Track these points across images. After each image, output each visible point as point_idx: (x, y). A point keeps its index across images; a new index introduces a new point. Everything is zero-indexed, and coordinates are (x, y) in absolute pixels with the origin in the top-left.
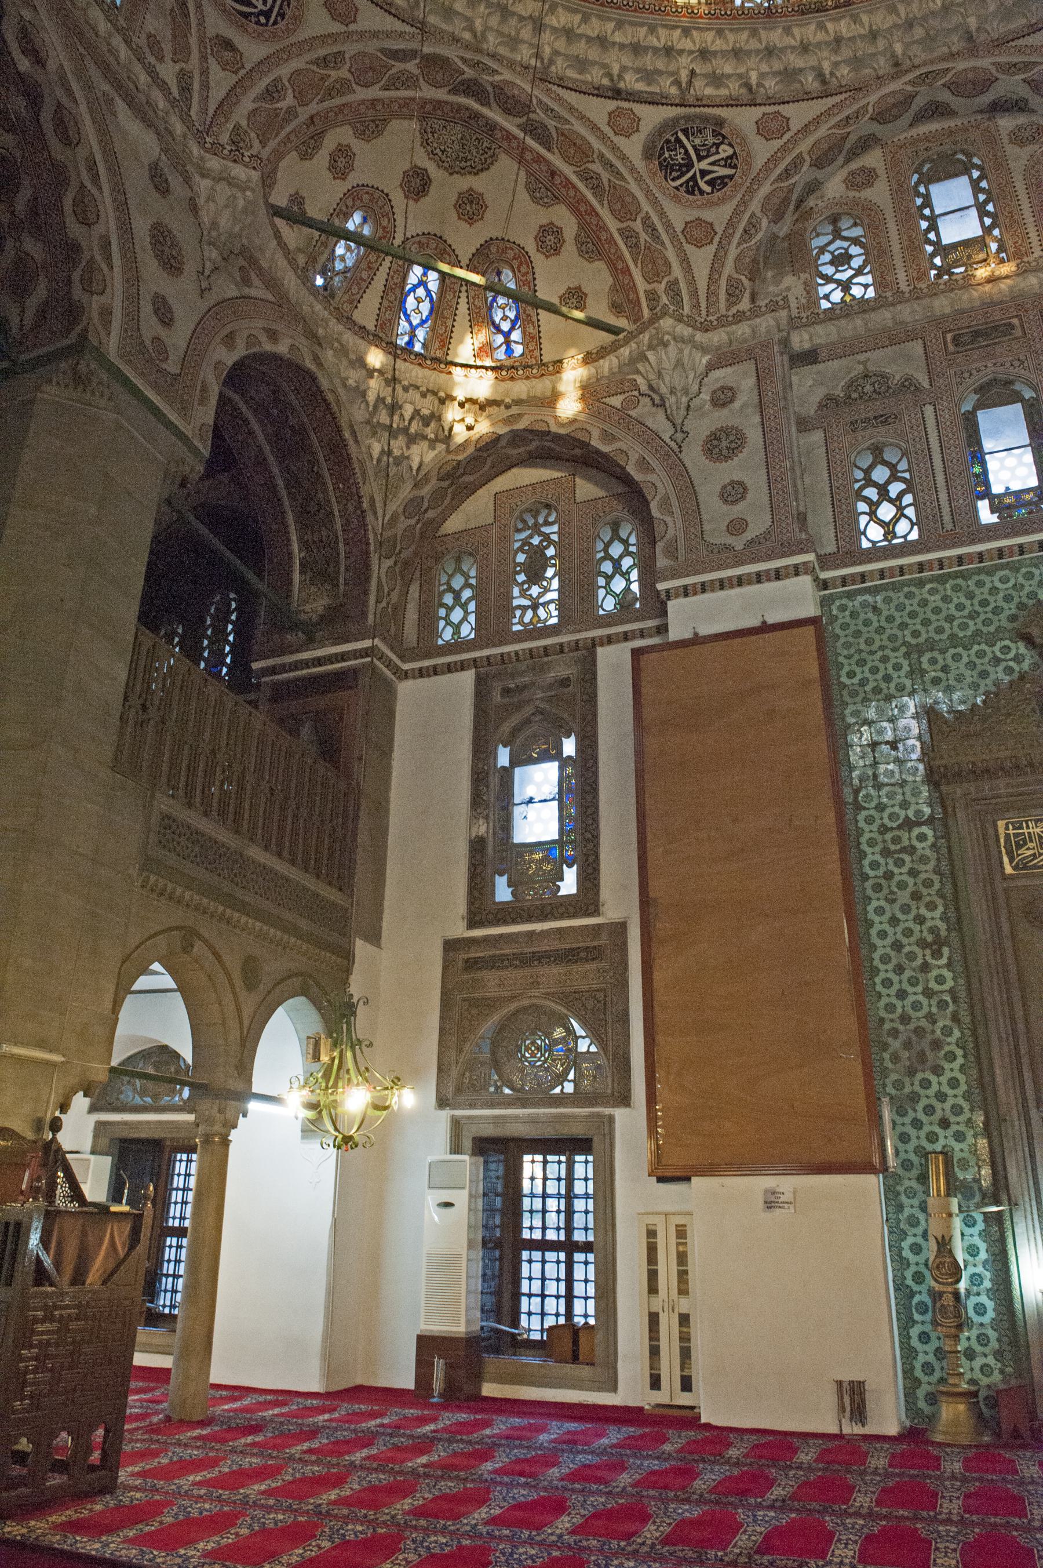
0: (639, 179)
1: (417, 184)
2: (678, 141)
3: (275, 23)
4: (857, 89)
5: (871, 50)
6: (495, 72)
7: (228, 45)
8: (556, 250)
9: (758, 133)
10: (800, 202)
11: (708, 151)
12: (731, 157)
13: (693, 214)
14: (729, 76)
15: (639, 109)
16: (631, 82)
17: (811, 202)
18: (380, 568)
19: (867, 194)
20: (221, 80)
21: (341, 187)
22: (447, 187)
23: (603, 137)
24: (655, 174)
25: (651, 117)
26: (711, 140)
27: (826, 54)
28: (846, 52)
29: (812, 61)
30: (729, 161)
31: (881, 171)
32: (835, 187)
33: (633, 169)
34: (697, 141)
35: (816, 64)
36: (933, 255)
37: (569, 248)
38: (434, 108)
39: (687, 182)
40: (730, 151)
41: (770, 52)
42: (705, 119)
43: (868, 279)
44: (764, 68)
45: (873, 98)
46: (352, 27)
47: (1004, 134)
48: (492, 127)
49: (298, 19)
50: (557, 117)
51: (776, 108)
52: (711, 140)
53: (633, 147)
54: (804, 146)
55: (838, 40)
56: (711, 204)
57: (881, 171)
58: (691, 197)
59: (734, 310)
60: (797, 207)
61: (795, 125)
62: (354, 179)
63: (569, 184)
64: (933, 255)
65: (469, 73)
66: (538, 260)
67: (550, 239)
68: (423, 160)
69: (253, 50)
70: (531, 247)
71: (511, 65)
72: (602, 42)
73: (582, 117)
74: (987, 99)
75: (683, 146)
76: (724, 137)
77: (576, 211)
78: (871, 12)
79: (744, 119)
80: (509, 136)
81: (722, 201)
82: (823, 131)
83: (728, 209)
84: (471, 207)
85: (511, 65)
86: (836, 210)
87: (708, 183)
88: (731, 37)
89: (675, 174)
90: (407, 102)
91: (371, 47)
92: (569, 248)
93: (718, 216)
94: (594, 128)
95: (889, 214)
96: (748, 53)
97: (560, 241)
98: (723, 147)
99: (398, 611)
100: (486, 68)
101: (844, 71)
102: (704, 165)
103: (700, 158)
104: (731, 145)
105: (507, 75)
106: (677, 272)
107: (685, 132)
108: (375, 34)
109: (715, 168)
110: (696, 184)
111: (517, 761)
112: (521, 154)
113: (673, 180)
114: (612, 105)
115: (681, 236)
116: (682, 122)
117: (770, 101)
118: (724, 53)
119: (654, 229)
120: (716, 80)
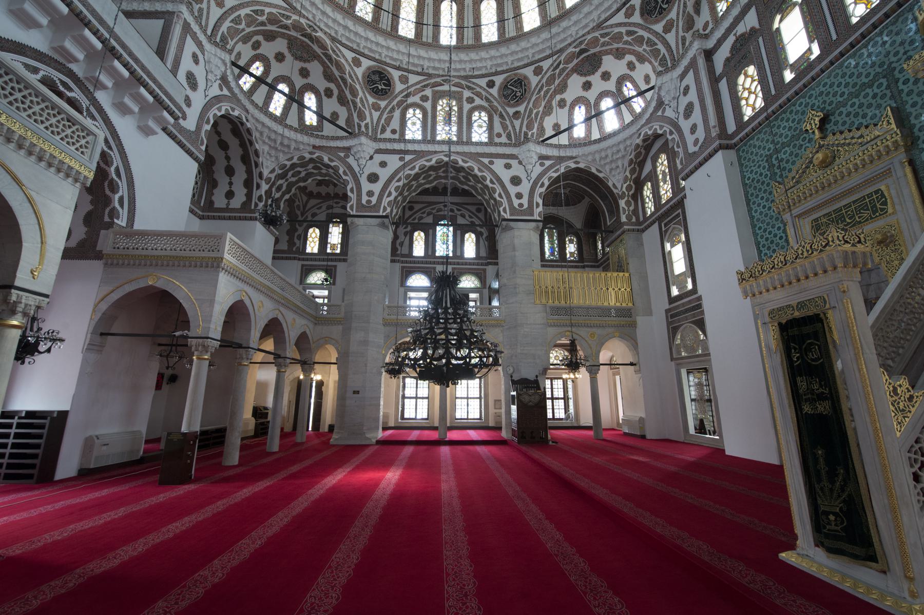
1: (587, 86)
8: (635, 67)
18: (622, 203)
21: (567, 108)
22: (595, 79)
37: (637, 64)
48: (594, 54)
62: (568, 104)
63: (623, 49)
65: (577, 50)
66: (632, 74)
67: (631, 66)
68: (584, 79)
70: (628, 72)
71: (588, 33)
77: (630, 53)
80: (600, 52)
84: (606, 76)
85: (588, 33)
90: (567, 74)
92: (637, 64)
97: (634, 64)
99: (635, 212)
100: (581, 43)
105: (589, 37)
111: (672, 246)
112: (607, 53)
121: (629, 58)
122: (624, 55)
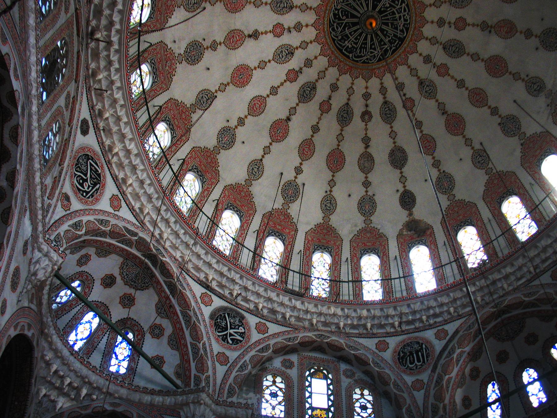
0: (205, 326)
2: (225, 316)
3: (89, 198)
4: (296, 329)
5: (305, 317)
6: (164, 256)
7: (67, 198)
9: (256, 328)
10: (264, 363)
11: (235, 326)
12: (242, 333)
13: (222, 350)
14: (251, 301)
15: (214, 297)
16: (214, 285)
17: (267, 365)
19: (288, 371)
20: (60, 212)
23: (196, 302)
24: (212, 326)
25: (217, 302)
26: (237, 323)
27: (289, 310)
28: (296, 314)
29: (283, 310)
30: (242, 334)
31: (296, 364)
32: (277, 363)
33: (204, 321)
34: (232, 321)
35: (284, 312)
36: (308, 409)
37: (165, 339)
38: (133, 258)
39: (223, 335)
40: (243, 331)
41: (269, 300)
42: (238, 313)
43: (283, 408)
44: (265, 304)
45: (301, 335)
46: (116, 213)
47: (342, 370)
49: (97, 200)
50: (182, 285)
51: (264, 321)
52: (237, 323)
53: (207, 311)
54: (272, 342)
55: (295, 307)
56: (230, 349)
57: (296, 364)
58: (223, 342)
59: (230, 400)
60: (261, 365)
61: (271, 332)
64: (308, 409)
66: (148, 336)
69: (76, 205)
72: (210, 265)
73: (191, 290)
74: (339, 354)
75: (226, 320)
76: (243, 324)
78: (309, 303)
79: (252, 320)
81: (235, 350)
82: (279, 339)
83: (236, 354)
86: (276, 372)
87: (231, 339)
88: (257, 288)
89: (219, 330)
91: (121, 224)
93: (233, 355)
94: (194, 296)
95: (296, 384)
96: (261, 296)
98: (241, 328)
101: (293, 320)
102: (232, 331)
103: (231, 328)
104: (244, 328)
106: (210, 372)
107: (228, 315)
108: (124, 220)
109: (236, 335)
110: (227, 338)
113: (219, 332)
114: (204, 290)
115: (215, 358)
116: (228, 310)
117: (263, 317)
118: (252, 292)
119: (206, 350)
120: (246, 300)
121: (166, 324)
122: (167, 317)
